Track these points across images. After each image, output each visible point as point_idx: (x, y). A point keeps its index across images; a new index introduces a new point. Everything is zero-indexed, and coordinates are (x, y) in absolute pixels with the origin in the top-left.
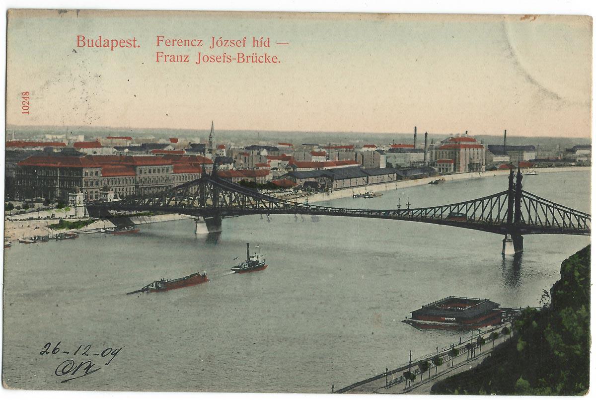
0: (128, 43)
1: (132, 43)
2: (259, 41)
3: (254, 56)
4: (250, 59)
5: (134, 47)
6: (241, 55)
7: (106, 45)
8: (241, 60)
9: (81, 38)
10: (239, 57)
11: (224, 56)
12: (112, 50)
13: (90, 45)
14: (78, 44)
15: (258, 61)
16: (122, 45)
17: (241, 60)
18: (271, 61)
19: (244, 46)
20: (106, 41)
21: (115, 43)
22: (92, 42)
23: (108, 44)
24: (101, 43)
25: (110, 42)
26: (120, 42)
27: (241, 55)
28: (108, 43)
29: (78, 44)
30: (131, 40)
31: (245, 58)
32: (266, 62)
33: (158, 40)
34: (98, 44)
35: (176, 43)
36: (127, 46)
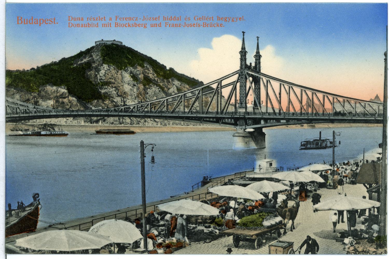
0: (50, 21)
1: (53, 20)
2: (167, 17)
3: (211, 24)
4: (209, 25)
5: (54, 23)
6: (205, 24)
7: (36, 22)
8: (205, 26)
9: (20, 18)
10: (204, 24)
11: (197, 24)
12: (40, 25)
13: (26, 22)
14: (18, 22)
15: (213, 26)
16: (47, 22)
17: (205, 26)
18: (219, 25)
19: (159, 20)
20: (36, 20)
21: (42, 21)
22: (27, 21)
23: (37, 22)
24: (32, 21)
25: (39, 21)
26: (45, 21)
27: (205, 24)
28: (37, 21)
29: (18, 22)
30: (52, 19)
31: (207, 25)
32: (217, 26)
33: (116, 18)
34: (31, 22)
35: (124, 19)
36: (50, 23)
